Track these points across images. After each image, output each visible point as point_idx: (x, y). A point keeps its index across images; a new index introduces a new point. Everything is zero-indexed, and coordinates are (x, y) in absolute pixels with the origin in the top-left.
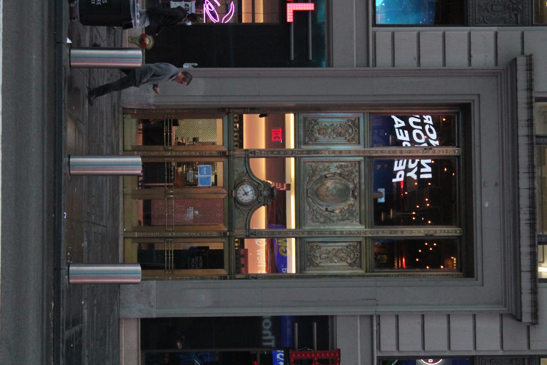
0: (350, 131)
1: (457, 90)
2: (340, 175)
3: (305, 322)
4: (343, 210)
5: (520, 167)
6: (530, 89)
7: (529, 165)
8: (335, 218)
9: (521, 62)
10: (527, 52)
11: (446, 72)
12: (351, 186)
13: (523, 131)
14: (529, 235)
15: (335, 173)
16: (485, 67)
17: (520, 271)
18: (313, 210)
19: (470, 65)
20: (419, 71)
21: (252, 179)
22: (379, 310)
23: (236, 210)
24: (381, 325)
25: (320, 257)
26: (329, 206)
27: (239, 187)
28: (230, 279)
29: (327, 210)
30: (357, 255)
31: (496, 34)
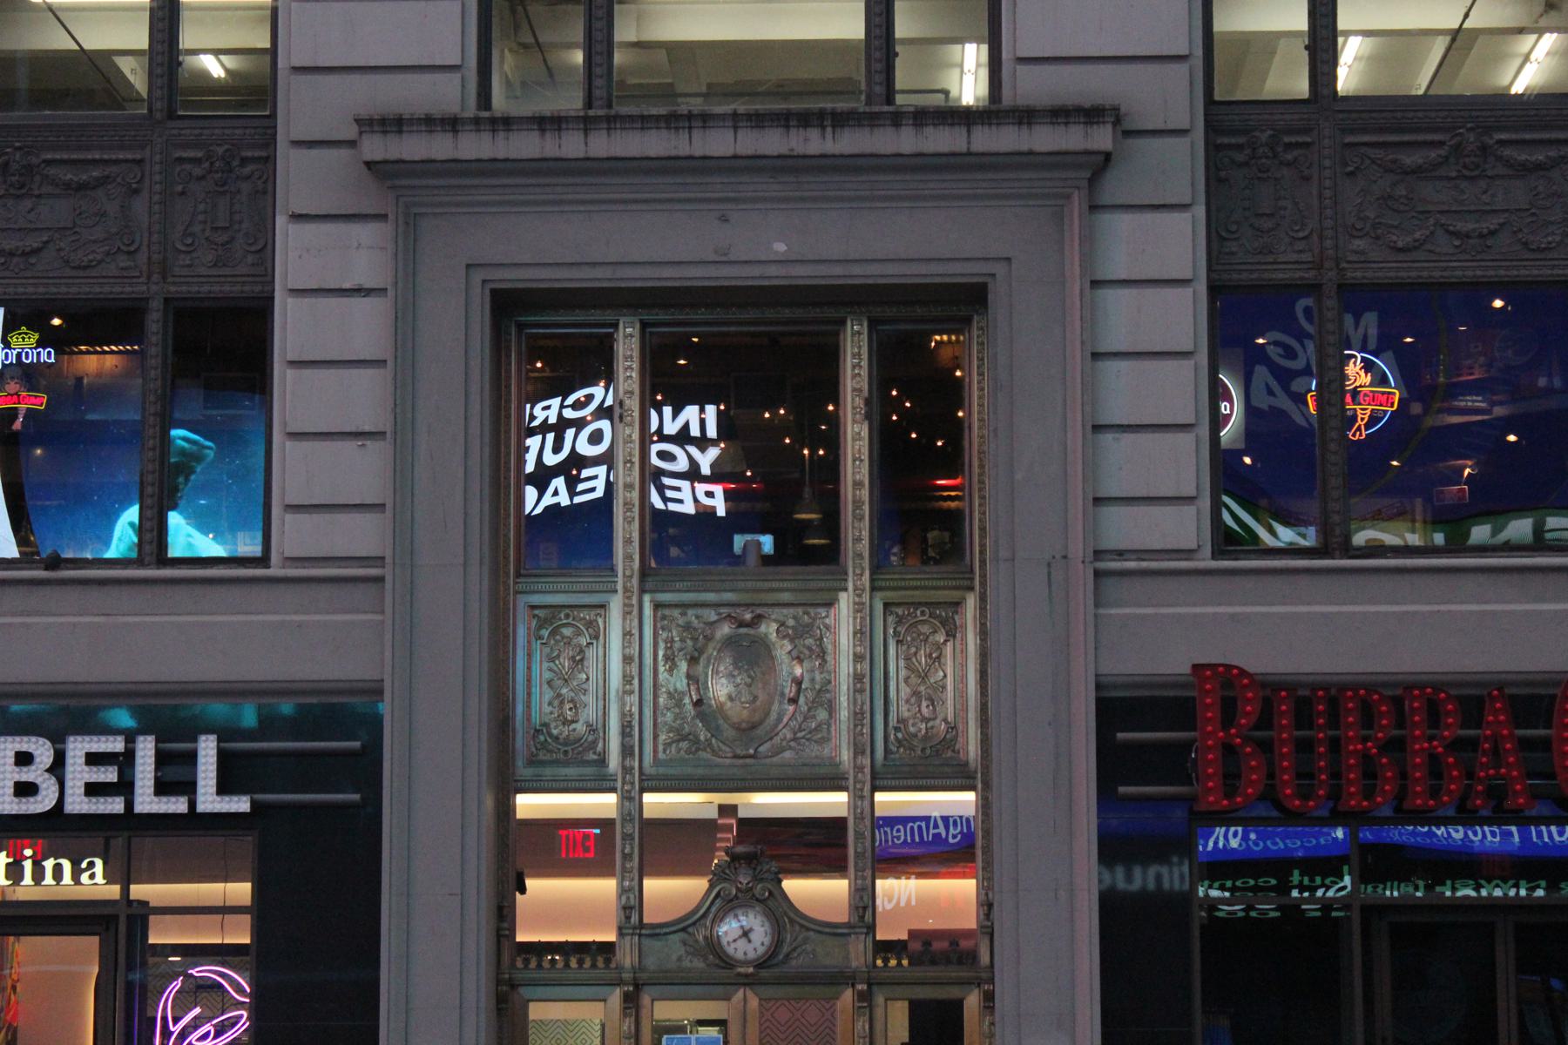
0: (567, 632)
1: (455, 331)
2: (693, 661)
3: (1114, 765)
4: (795, 654)
5: (673, 153)
6: (452, 124)
7: (668, 128)
8: (818, 677)
9: (376, 147)
10: (350, 132)
11: (402, 361)
12: (726, 629)
13: (571, 145)
14: (867, 129)
15: (689, 676)
17: (969, 154)
18: (795, 739)
19: (381, 291)
20: (399, 435)
21: (704, 916)
22: (1081, 554)
23: (794, 962)
24: (1122, 547)
25: (926, 720)
26: (782, 694)
27: (725, 952)
28: (991, 981)
29: (794, 701)
30: (923, 613)
31: (297, 217)
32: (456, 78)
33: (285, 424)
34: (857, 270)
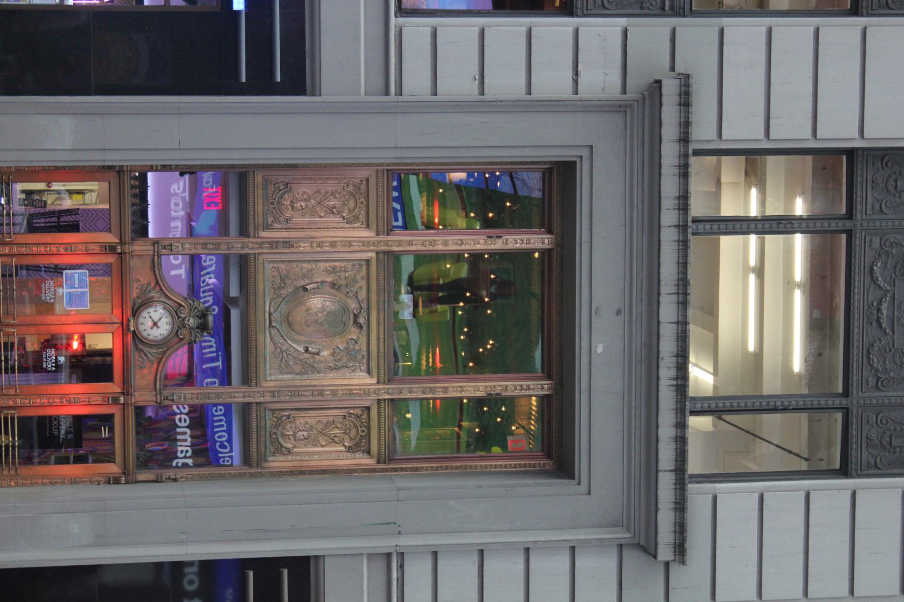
0: (352, 204)
1: (549, 139)
2: (333, 285)
3: (268, 568)
4: (337, 351)
5: (662, 283)
6: (684, 139)
7: (678, 280)
8: (322, 365)
9: (670, 89)
10: (680, 68)
11: (530, 105)
12: (353, 305)
13: (669, 217)
14: (674, 406)
15: (323, 282)
16: (602, 96)
17: (657, 471)
18: (282, 351)
19: (576, 92)
21: (166, 295)
22: (401, 544)
23: (137, 354)
24: (406, 568)
25: (294, 436)
26: (311, 343)
27: (143, 310)
28: (127, 482)
29: (307, 350)
30: (363, 431)
31: (625, 32)
32: (714, 136)
33: (490, 26)
34: (584, 397)
